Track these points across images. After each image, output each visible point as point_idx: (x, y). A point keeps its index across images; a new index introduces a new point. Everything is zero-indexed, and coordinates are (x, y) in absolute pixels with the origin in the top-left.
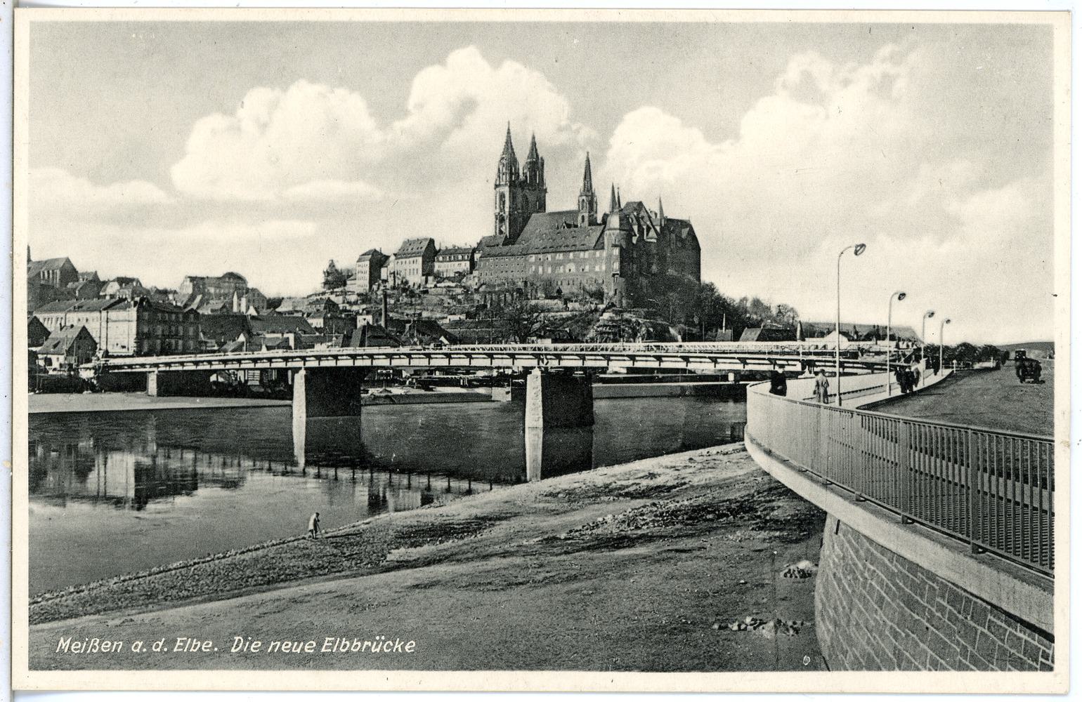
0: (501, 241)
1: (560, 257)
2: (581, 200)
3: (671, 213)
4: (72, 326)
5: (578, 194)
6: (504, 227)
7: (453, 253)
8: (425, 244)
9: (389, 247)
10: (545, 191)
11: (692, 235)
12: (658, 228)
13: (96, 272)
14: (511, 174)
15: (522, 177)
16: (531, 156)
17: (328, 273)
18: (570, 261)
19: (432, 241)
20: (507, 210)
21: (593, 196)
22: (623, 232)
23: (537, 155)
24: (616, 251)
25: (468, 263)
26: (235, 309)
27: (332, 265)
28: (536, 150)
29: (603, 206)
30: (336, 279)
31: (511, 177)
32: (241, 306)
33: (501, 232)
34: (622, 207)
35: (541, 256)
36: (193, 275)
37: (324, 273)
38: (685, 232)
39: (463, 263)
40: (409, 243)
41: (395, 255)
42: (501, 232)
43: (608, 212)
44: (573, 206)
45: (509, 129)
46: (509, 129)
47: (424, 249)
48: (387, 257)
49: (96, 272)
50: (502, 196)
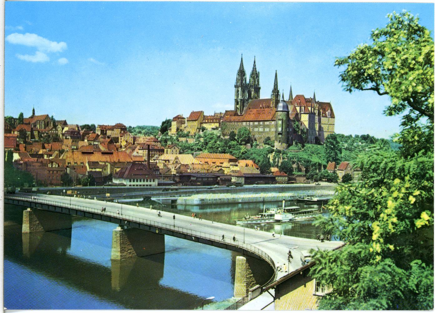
0: (233, 114)
1: (256, 123)
2: (272, 93)
5: (272, 91)
6: (238, 106)
9: (186, 115)
10: (260, 88)
12: (310, 108)
13: (65, 121)
14: (242, 80)
15: (248, 81)
16: (253, 71)
18: (260, 125)
20: (240, 97)
21: (278, 92)
22: (284, 113)
23: (256, 71)
24: (280, 122)
25: (218, 124)
28: (256, 69)
31: (242, 82)
35: (248, 123)
36: (101, 124)
39: (216, 124)
40: (193, 113)
41: (187, 118)
42: (237, 108)
44: (269, 97)
45: (242, 59)
46: (242, 59)
49: (65, 121)
50: (238, 91)
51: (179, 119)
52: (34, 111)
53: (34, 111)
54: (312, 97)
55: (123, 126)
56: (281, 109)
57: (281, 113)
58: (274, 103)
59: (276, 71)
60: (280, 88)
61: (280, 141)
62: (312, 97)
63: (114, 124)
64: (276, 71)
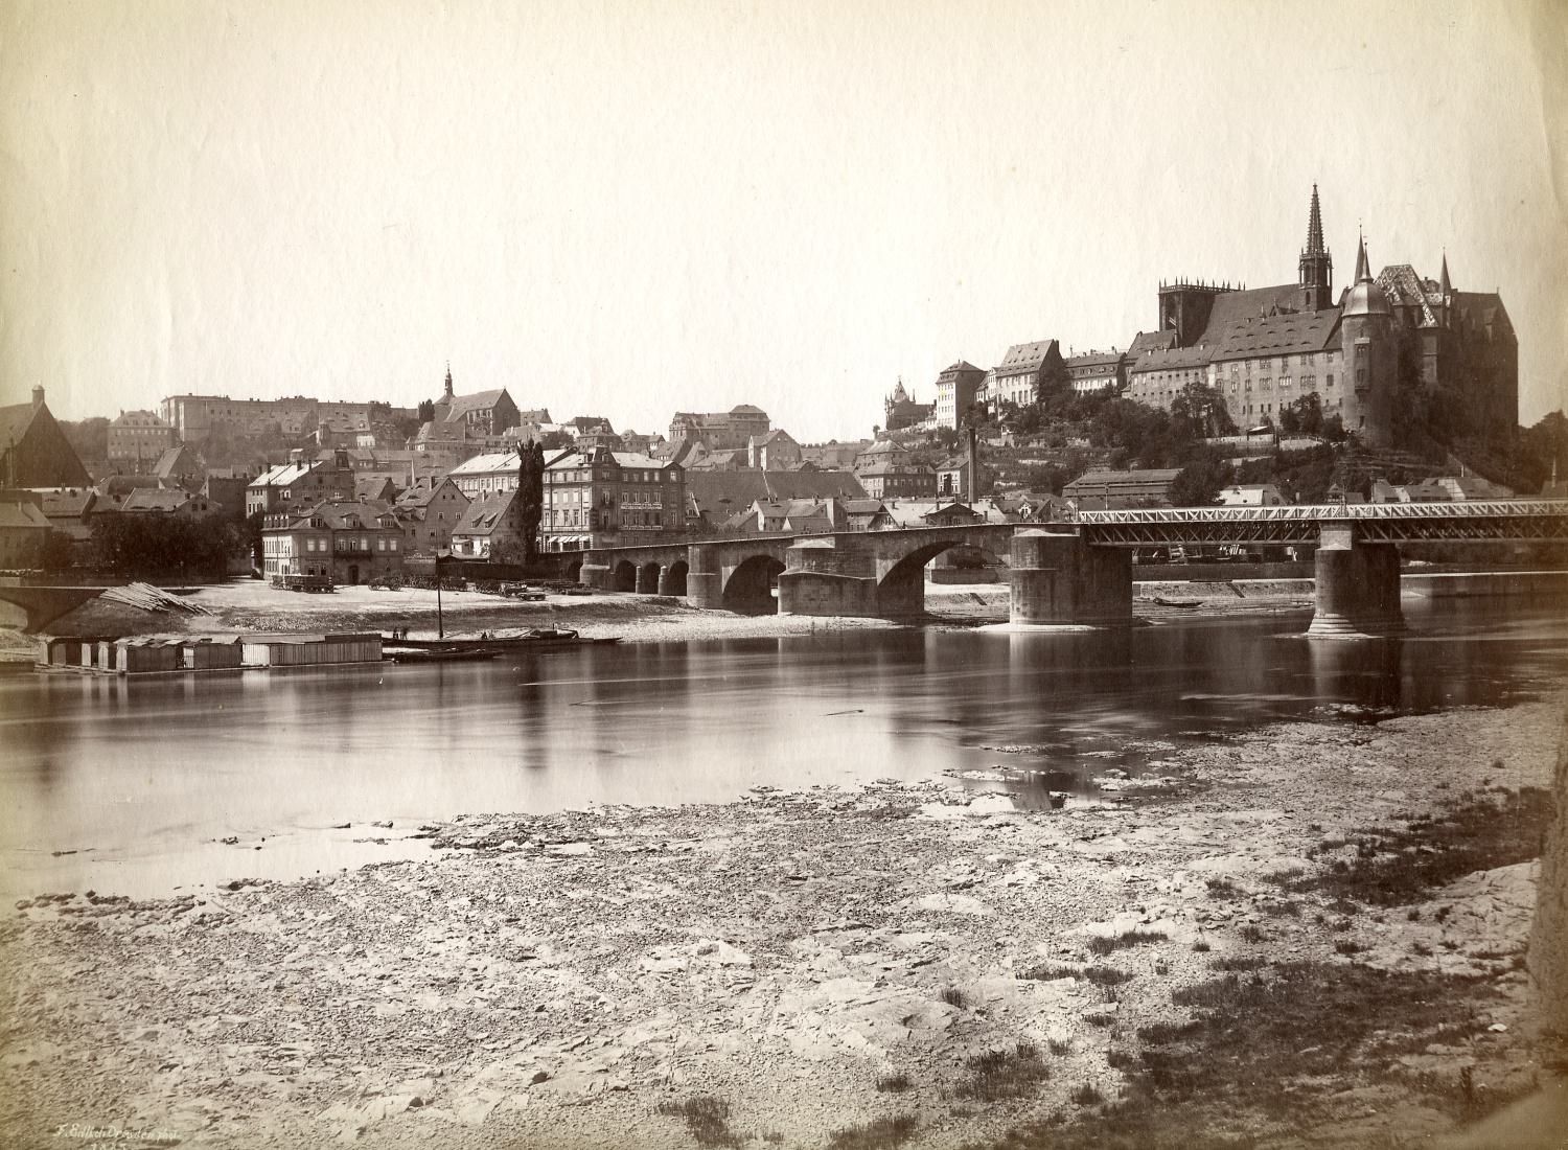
3: (1463, 283)
4: (501, 491)
7: (1092, 364)
8: (1043, 352)
11: (1501, 318)
12: (1440, 312)
13: (546, 411)
17: (892, 404)
19: (1055, 345)
26: (751, 463)
27: (901, 391)
29: (1342, 277)
30: (905, 413)
32: (760, 460)
33: (1169, 326)
34: (1375, 274)
37: (887, 402)
38: (1489, 314)
41: (996, 369)
43: (1351, 285)
47: (1042, 359)
48: (982, 374)
51: (967, 379)
52: (449, 382)
53: (449, 382)
54: (1437, 277)
55: (753, 415)
56: (1364, 310)
57: (1361, 320)
58: (1313, 299)
59: (1315, 186)
60: (1328, 242)
61: (1362, 418)
62: (1437, 277)
63: (726, 408)
64: (1315, 186)
